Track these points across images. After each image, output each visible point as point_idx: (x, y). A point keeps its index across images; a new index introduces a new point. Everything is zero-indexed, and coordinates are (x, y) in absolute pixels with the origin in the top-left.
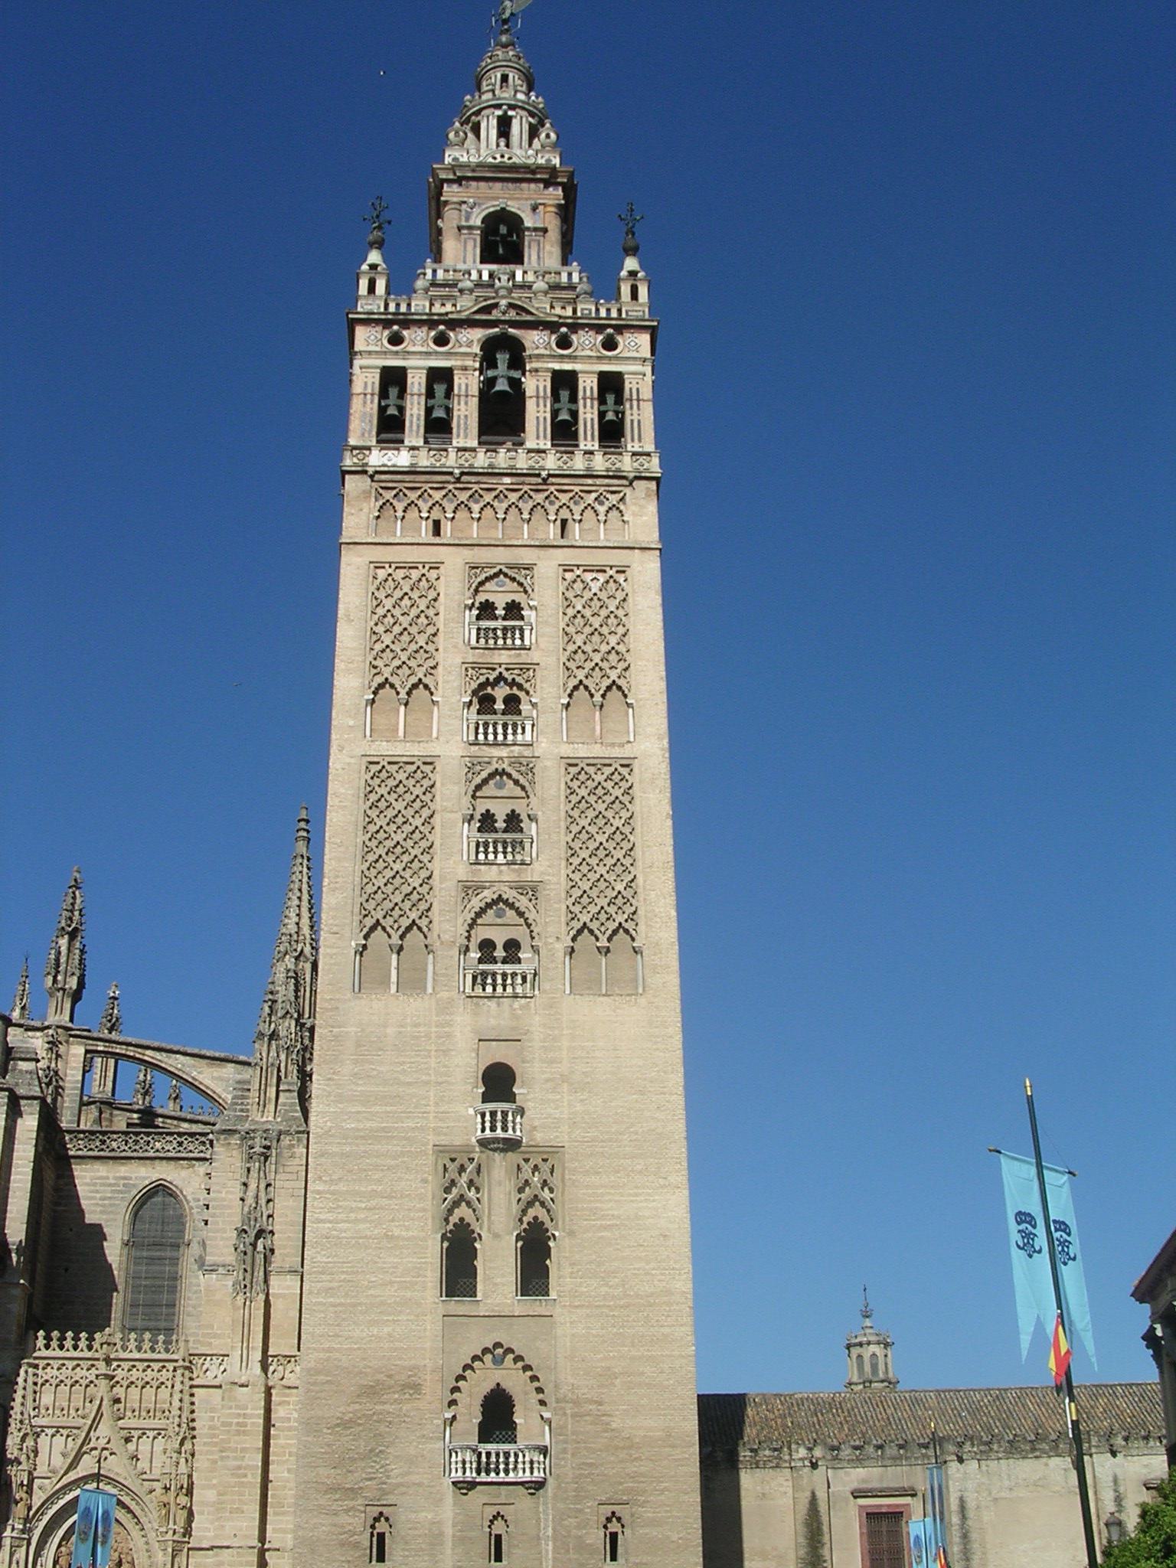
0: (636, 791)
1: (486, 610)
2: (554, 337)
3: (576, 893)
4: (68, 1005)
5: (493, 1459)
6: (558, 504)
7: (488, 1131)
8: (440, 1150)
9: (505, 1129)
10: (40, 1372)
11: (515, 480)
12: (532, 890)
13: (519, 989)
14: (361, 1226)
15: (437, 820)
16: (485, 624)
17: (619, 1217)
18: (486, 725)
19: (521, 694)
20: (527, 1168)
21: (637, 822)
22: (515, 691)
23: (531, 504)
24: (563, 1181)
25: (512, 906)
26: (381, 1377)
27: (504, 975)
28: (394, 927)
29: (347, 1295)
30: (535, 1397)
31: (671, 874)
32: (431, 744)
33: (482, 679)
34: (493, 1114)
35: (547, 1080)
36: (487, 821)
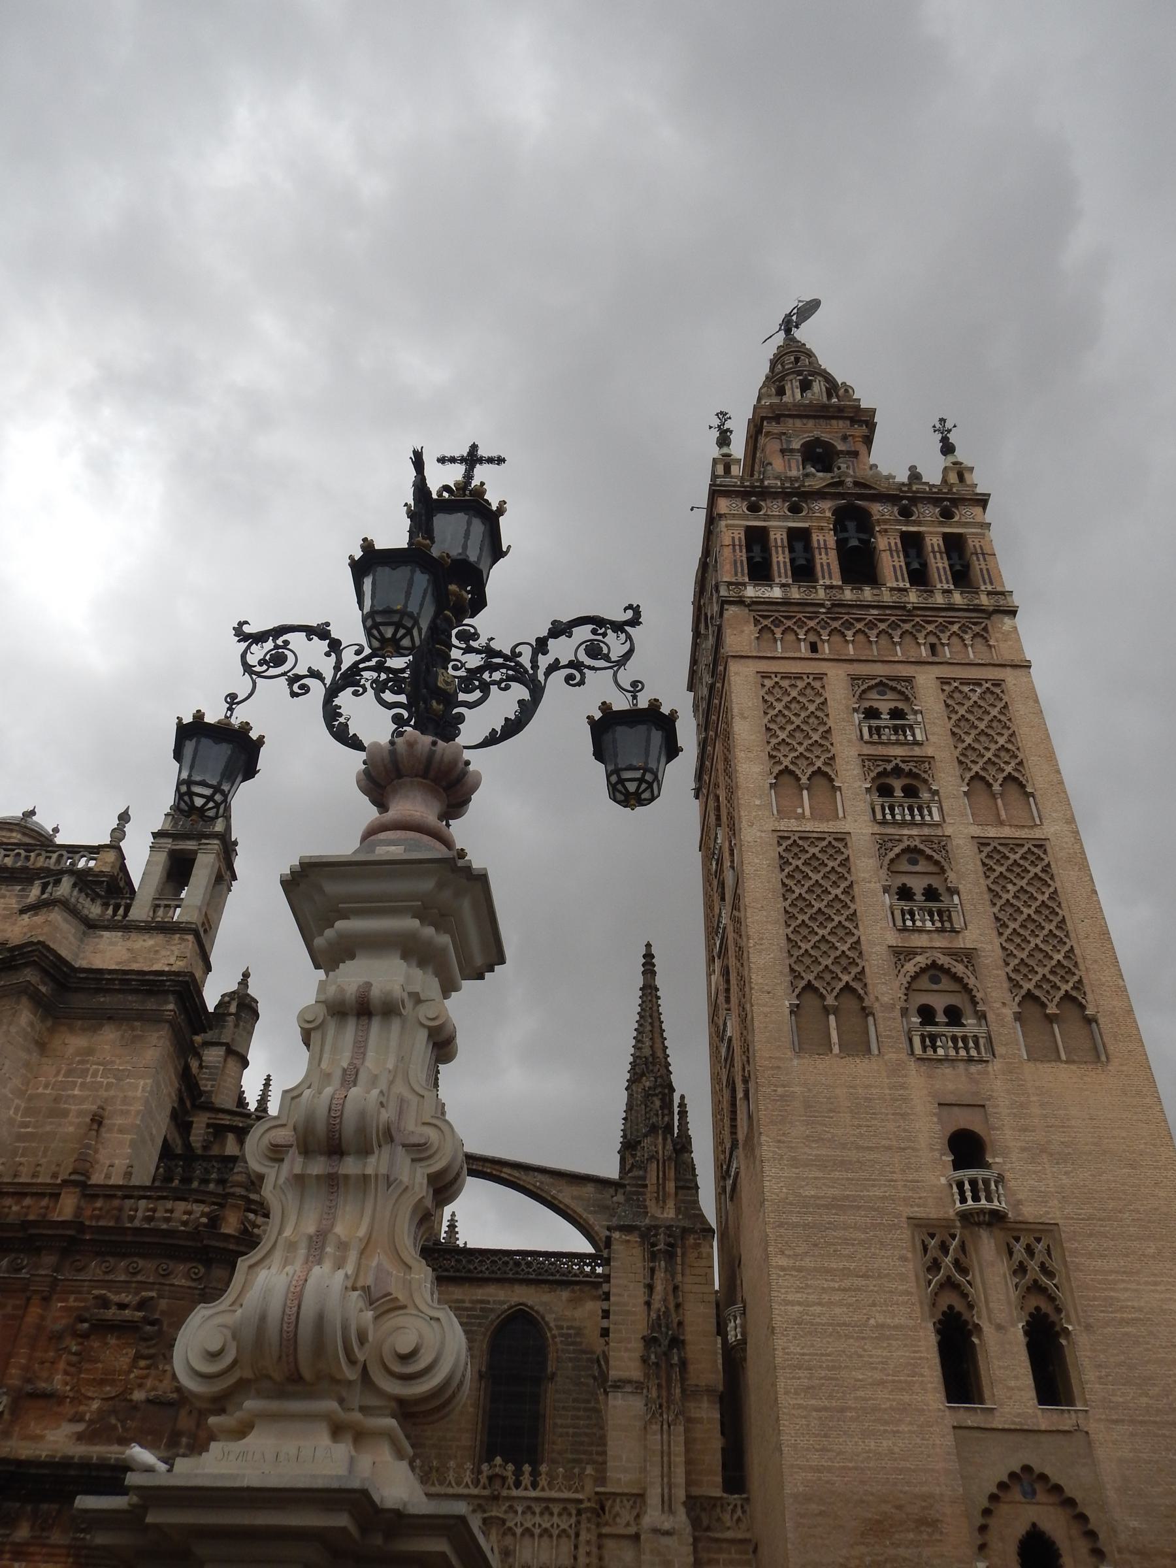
0: (1054, 869)
2: (896, 509)
6: (924, 632)
7: (970, 1202)
8: (916, 1223)
9: (989, 1199)
13: (973, 1053)
14: (838, 1311)
16: (875, 723)
17: (1140, 1310)
20: (1019, 1248)
24: (1065, 1263)
25: (947, 972)
29: (830, 1397)
30: (1083, 1547)
32: (839, 823)
33: (880, 769)
34: (973, 1183)
35: (1023, 1149)
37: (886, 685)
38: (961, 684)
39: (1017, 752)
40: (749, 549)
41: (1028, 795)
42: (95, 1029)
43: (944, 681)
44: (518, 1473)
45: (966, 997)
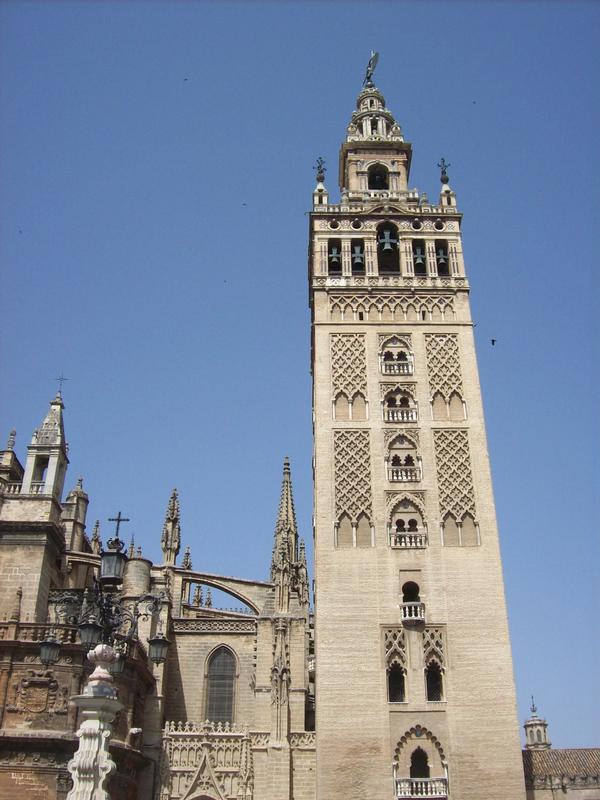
0: (469, 445)
1: (388, 356)
3: (444, 496)
4: (173, 556)
5: (419, 786)
8: (384, 627)
9: (416, 615)
10: (173, 743)
12: (421, 494)
14: (346, 666)
15: (371, 461)
16: (388, 363)
20: (428, 635)
21: (471, 460)
23: (407, 304)
26: (359, 744)
27: (410, 538)
28: (353, 516)
31: (490, 486)
34: (410, 608)
36: (396, 461)
40: (330, 252)
41: (463, 402)
42: (13, 550)
44: (216, 726)
45: (418, 514)
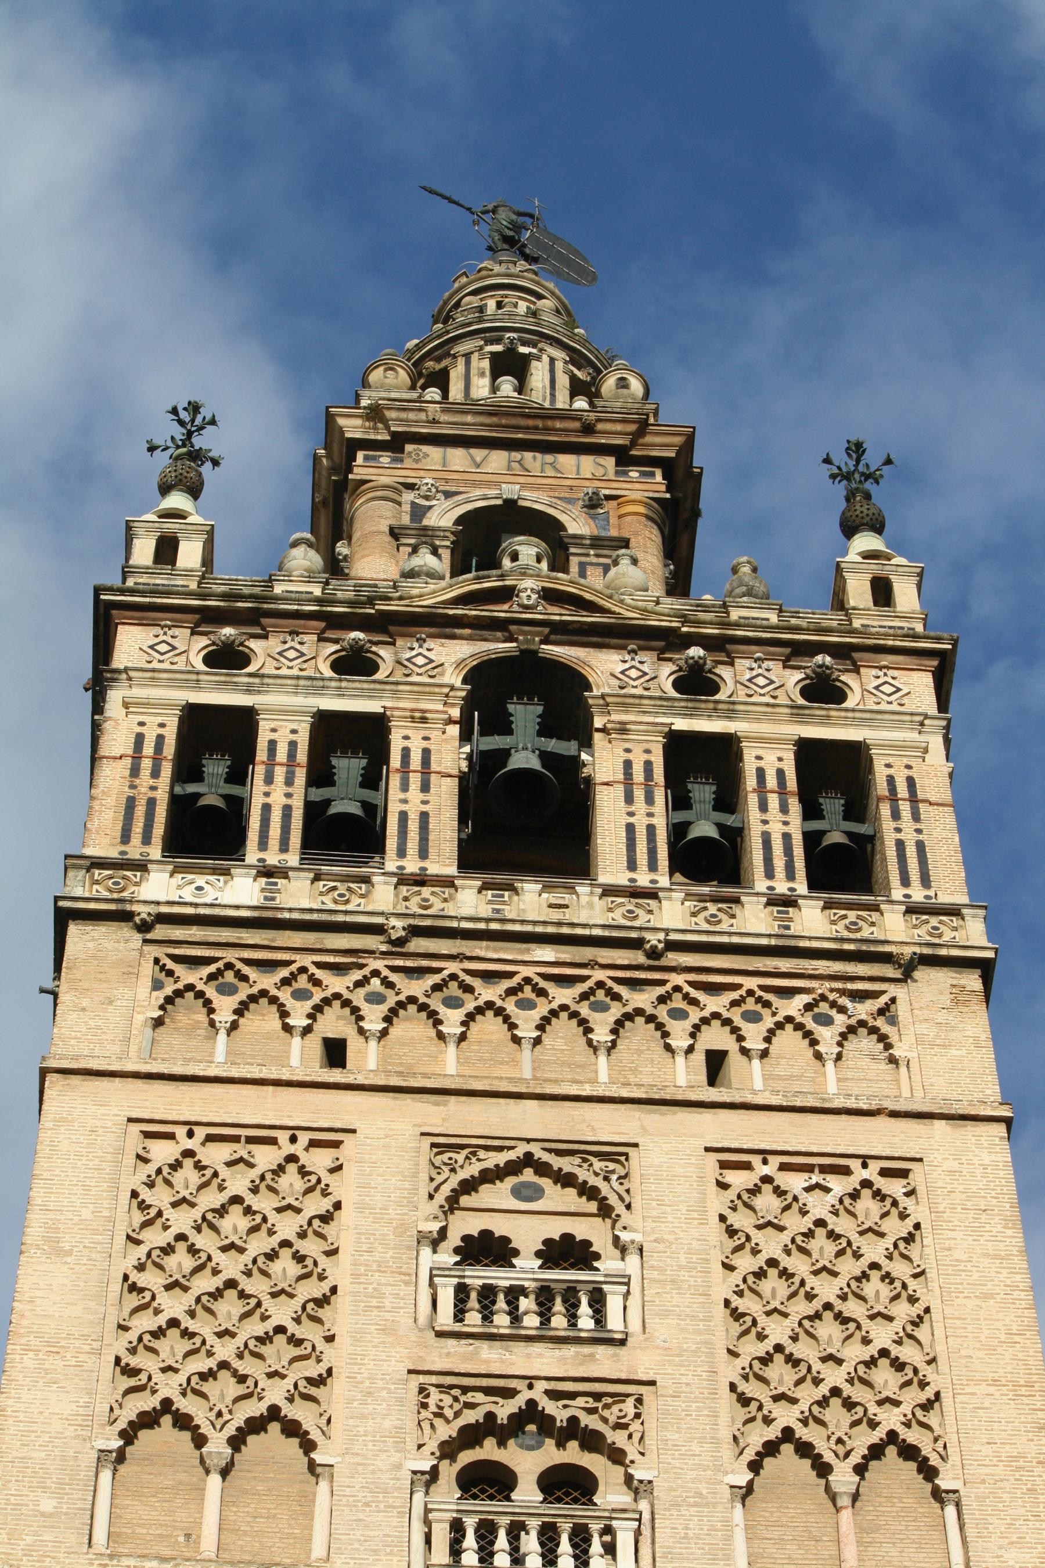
11: (566, 954)
16: (477, 1276)
18: (486, 1531)
19: (594, 1462)
22: (573, 1454)
33: (471, 1417)
37: (543, 1169)
38: (783, 1167)
39: (925, 1370)
43: (732, 1159)
